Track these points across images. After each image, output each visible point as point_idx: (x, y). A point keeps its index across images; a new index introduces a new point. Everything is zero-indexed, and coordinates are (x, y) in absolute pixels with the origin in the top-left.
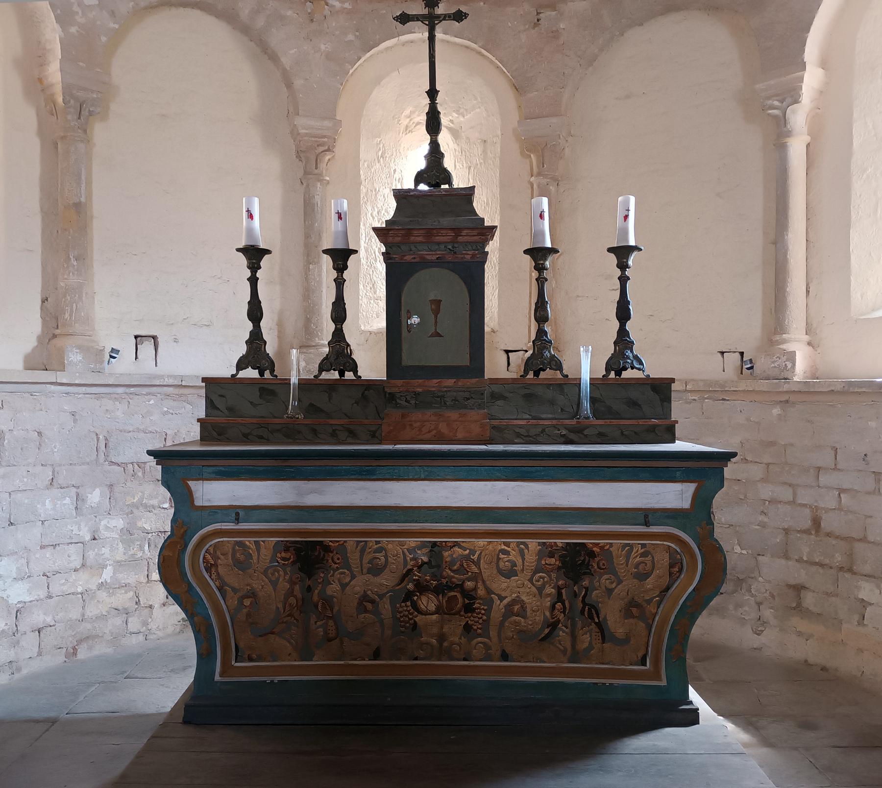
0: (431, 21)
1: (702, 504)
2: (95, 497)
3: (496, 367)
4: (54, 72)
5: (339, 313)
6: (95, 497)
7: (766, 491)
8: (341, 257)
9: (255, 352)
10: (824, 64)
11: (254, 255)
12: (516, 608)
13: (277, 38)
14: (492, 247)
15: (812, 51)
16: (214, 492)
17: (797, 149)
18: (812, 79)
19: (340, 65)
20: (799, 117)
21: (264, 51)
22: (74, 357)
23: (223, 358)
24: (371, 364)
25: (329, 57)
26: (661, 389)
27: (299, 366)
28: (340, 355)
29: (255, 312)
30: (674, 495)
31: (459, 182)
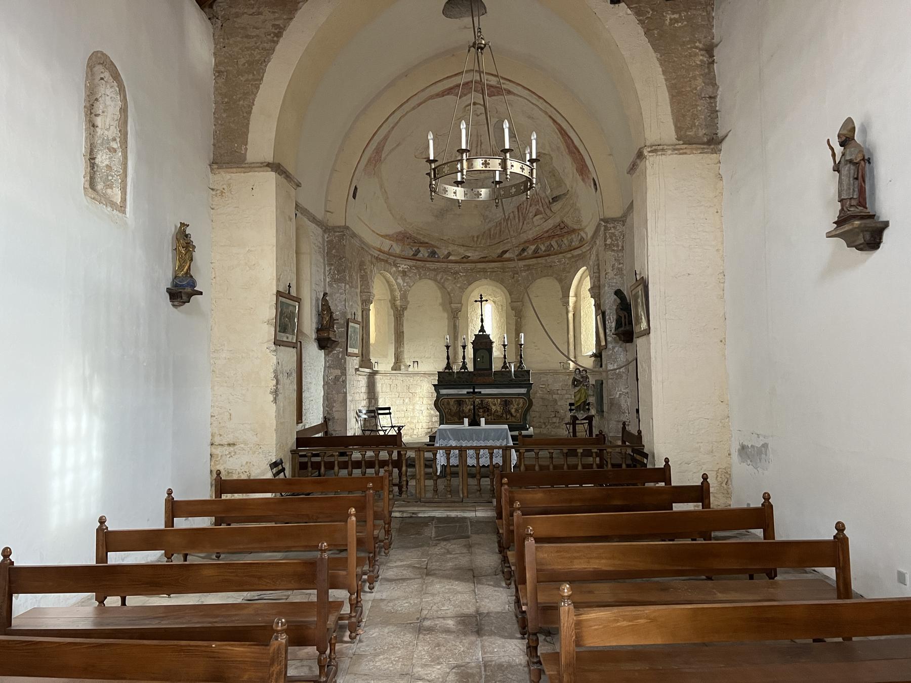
0: (481, 301)
1: (528, 391)
2: (407, 400)
3: (496, 366)
4: (398, 303)
5: (464, 358)
6: (407, 400)
7: (567, 396)
8: (464, 347)
9: (448, 366)
10: (576, 296)
11: (448, 347)
12: (496, 411)
13: (446, 284)
14: (494, 345)
15: (572, 293)
16: (443, 392)
17: (571, 315)
18: (572, 300)
19: (463, 289)
20: (571, 308)
21: (442, 287)
22: (403, 367)
23: (441, 367)
24: (470, 367)
25: (460, 288)
26: (528, 372)
27: (456, 368)
28: (464, 366)
29: (448, 358)
30: (523, 391)
31: (487, 333)
